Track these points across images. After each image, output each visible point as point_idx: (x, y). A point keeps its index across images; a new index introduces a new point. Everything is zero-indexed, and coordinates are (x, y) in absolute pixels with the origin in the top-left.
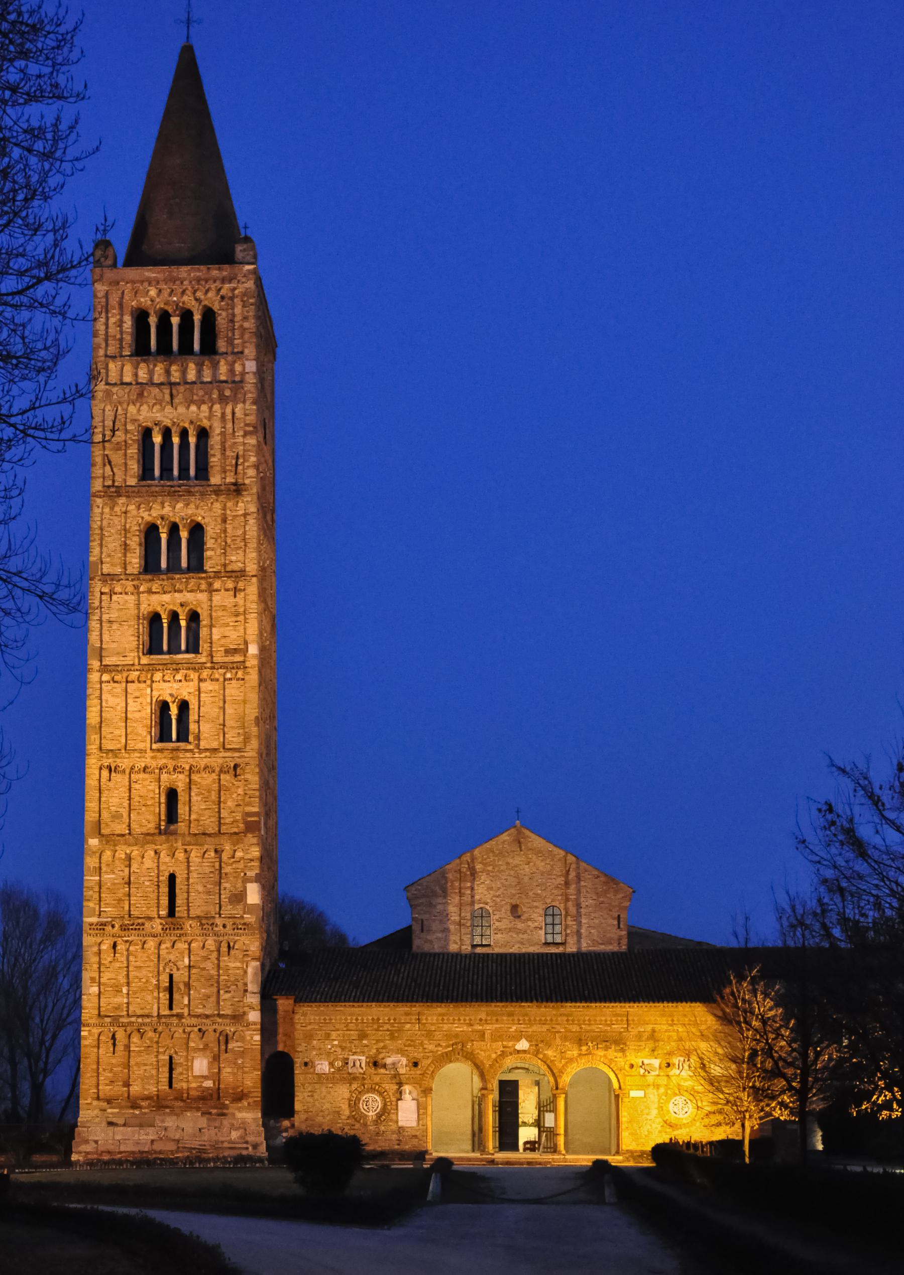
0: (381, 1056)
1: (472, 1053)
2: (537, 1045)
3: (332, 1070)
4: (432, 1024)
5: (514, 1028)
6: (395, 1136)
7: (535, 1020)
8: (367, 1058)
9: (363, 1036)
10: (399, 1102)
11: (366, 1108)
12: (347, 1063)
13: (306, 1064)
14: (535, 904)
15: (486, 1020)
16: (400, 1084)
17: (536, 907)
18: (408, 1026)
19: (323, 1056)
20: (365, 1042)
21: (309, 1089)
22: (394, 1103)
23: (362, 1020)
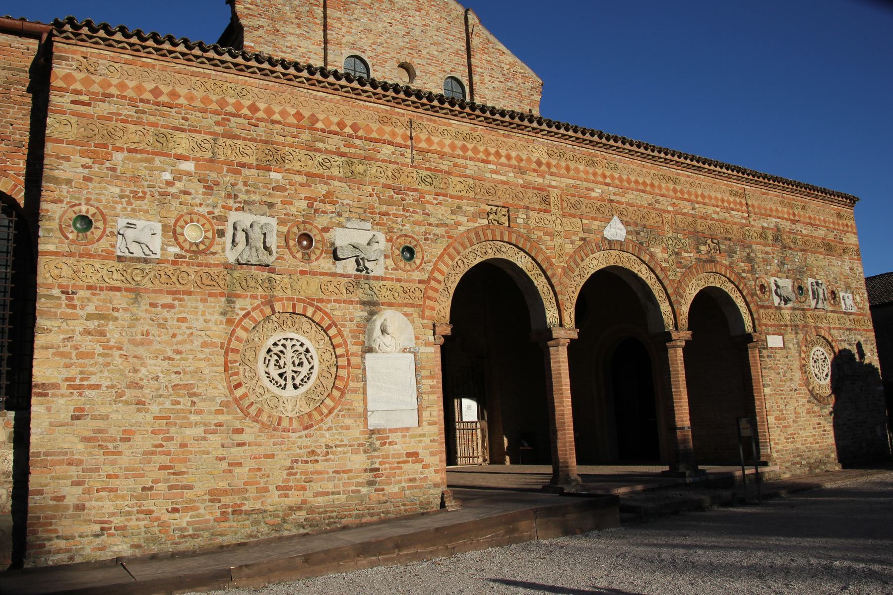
0: (321, 221)
1: (528, 239)
2: (638, 233)
3: (174, 250)
4: (442, 155)
5: (597, 192)
6: (359, 461)
7: (629, 181)
8: (281, 222)
9: (271, 158)
10: (367, 355)
11: (274, 372)
12: (221, 233)
13: (85, 222)
14: (432, 69)
15: (549, 165)
16: (372, 306)
17: (434, 74)
18: (386, 151)
19: (145, 204)
20: (273, 175)
21: (91, 309)
22: (354, 360)
23: (269, 111)
